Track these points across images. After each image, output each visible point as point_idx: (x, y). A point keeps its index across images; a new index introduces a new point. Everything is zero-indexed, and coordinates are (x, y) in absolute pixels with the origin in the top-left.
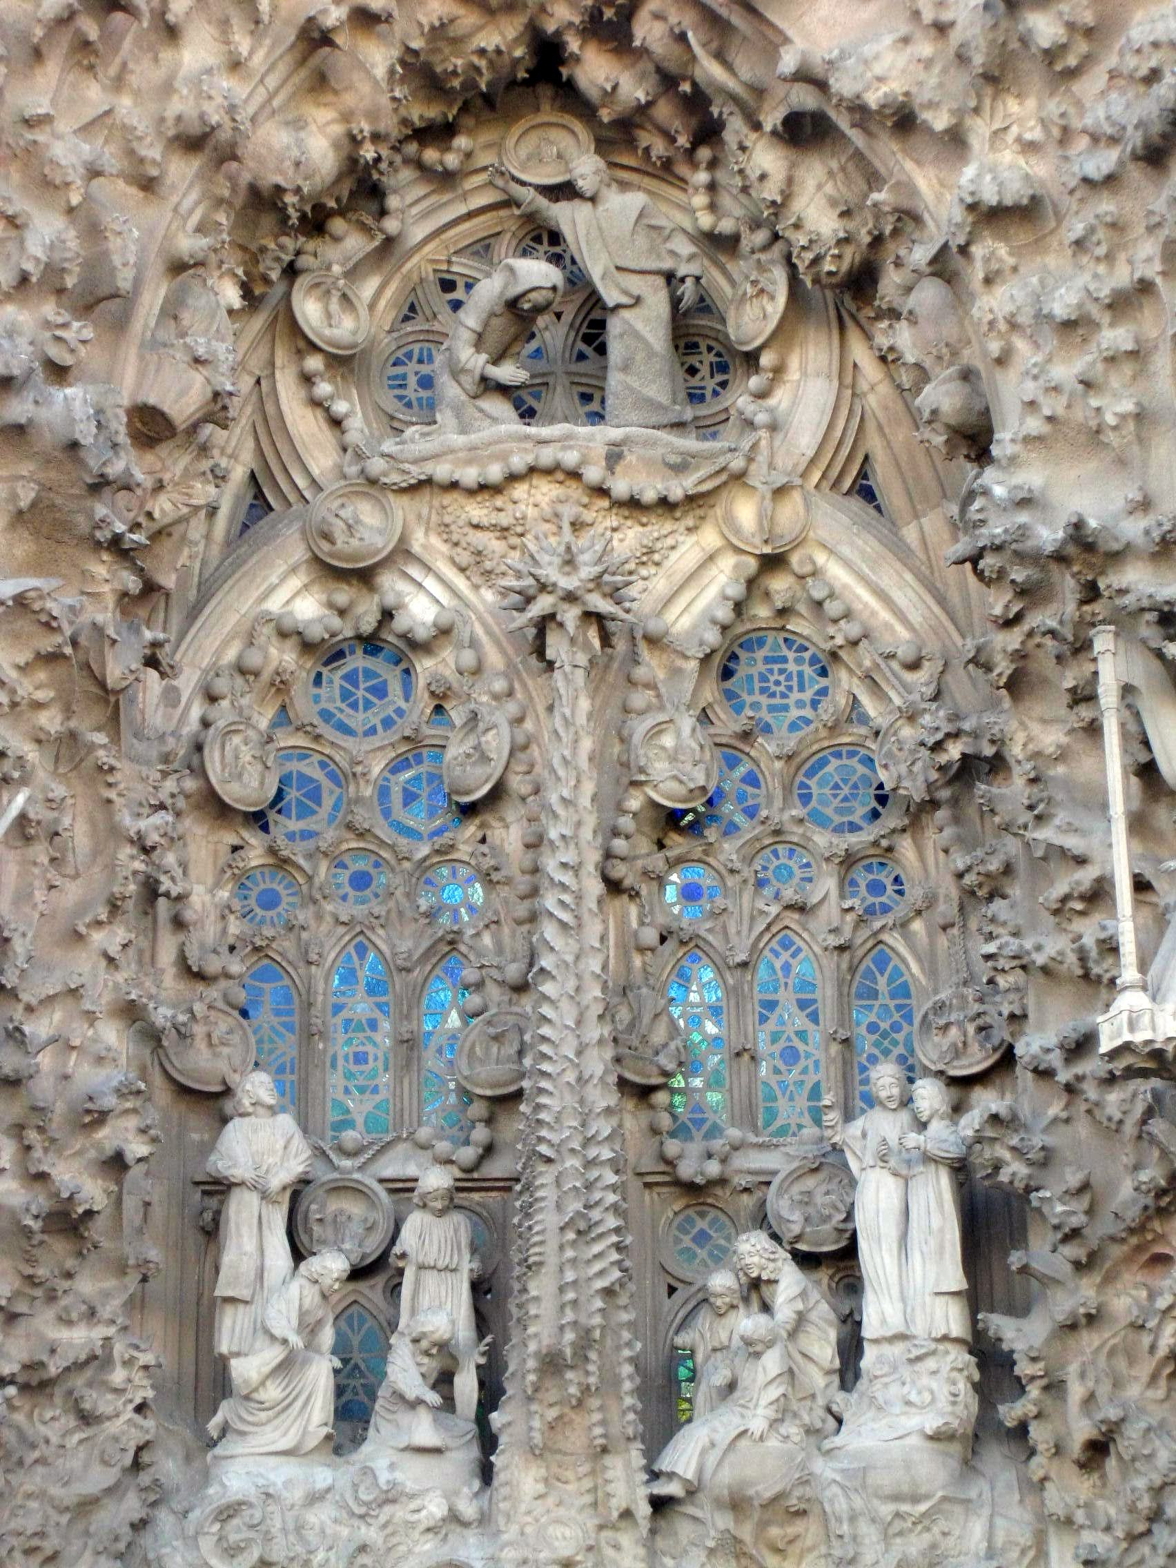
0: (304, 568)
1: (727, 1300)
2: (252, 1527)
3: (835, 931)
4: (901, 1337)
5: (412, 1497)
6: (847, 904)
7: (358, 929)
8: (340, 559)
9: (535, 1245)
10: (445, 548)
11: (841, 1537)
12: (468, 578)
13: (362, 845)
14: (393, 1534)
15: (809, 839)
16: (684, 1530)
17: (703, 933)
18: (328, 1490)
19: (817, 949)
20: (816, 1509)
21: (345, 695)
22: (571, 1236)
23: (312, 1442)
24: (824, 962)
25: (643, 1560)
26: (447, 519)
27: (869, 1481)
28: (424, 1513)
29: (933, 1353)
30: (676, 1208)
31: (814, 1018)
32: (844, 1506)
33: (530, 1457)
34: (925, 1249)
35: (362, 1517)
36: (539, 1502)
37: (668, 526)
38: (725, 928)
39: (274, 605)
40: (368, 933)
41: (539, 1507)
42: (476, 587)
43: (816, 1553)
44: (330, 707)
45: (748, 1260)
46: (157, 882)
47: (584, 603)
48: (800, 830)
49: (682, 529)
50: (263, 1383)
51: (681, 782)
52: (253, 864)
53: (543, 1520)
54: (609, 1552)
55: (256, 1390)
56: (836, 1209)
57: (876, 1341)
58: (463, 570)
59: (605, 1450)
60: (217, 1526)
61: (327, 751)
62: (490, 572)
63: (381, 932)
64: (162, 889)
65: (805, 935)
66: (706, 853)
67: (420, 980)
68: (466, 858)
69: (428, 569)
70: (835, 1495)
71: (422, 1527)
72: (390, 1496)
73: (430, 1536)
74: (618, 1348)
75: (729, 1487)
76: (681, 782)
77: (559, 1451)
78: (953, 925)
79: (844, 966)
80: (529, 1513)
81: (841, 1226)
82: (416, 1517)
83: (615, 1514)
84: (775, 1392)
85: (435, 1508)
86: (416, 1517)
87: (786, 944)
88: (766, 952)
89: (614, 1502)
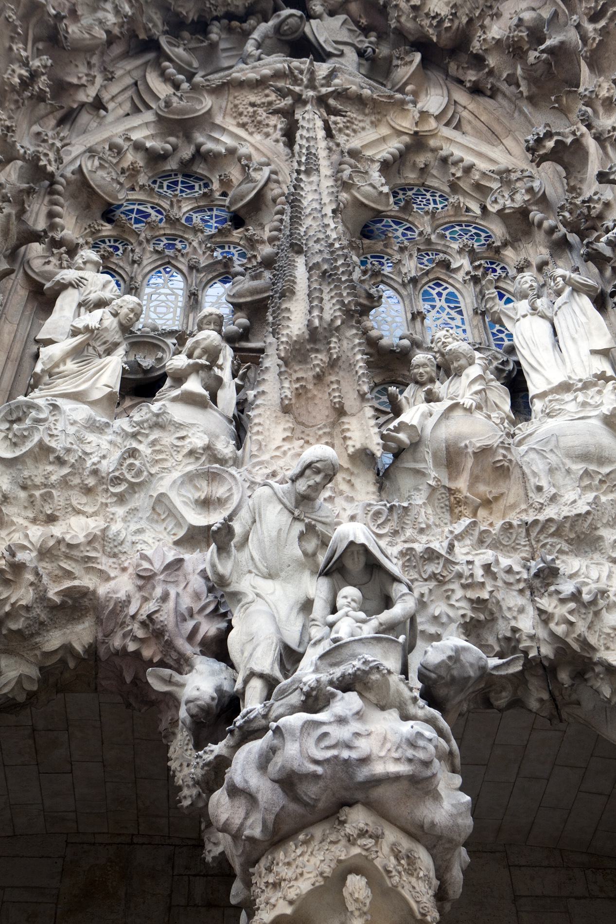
0: (153, 125)
1: (428, 369)
2: (38, 421)
3: (468, 273)
4: (565, 387)
5: (179, 426)
6: (477, 263)
7: (167, 260)
8: (173, 113)
9: (289, 280)
10: (234, 122)
11: (539, 489)
12: (247, 130)
13: (173, 232)
14: (160, 452)
15: (448, 247)
16: (405, 482)
17: (385, 273)
18: (107, 425)
19: (457, 286)
20: (516, 473)
21: (169, 187)
22: (316, 273)
23: (97, 395)
24: (463, 291)
25: (374, 493)
26: (237, 102)
27: (561, 444)
28: (188, 440)
29: (595, 385)
30: (377, 381)
31: (460, 313)
32: (541, 466)
33: (280, 414)
34: (576, 336)
35: (134, 436)
36: (285, 443)
37: (360, 118)
38: (400, 272)
39: (136, 136)
40: (173, 262)
41: (286, 446)
42: (251, 134)
43: (518, 510)
44: (161, 191)
45: (443, 340)
46: (39, 159)
47: (319, 92)
48: (443, 243)
49: (368, 122)
50: (63, 360)
51: (374, 187)
52: (104, 234)
53: (290, 453)
54: (344, 487)
55: (57, 365)
56: (496, 358)
57: (542, 395)
58: (243, 126)
59: (340, 412)
60: (7, 425)
61: (156, 201)
62: (260, 122)
63: (181, 259)
64: (42, 163)
65: (450, 281)
66: (386, 246)
67: (205, 280)
68: (237, 241)
69: (223, 130)
70: (533, 460)
71: (186, 451)
72: (160, 420)
73: (192, 460)
74: (353, 348)
75: (446, 441)
76: (374, 187)
77: (303, 424)
78: (546, 263)
79: (478, 289)
80: (278, 448)
81: (500, 366)
82: (179, 443)
83: (351, 450)
84: (477, 387)
85: (198, 441)
86: (179, 443)
87: (439, 285)
88: (426, 287)
89: (349, 443)
